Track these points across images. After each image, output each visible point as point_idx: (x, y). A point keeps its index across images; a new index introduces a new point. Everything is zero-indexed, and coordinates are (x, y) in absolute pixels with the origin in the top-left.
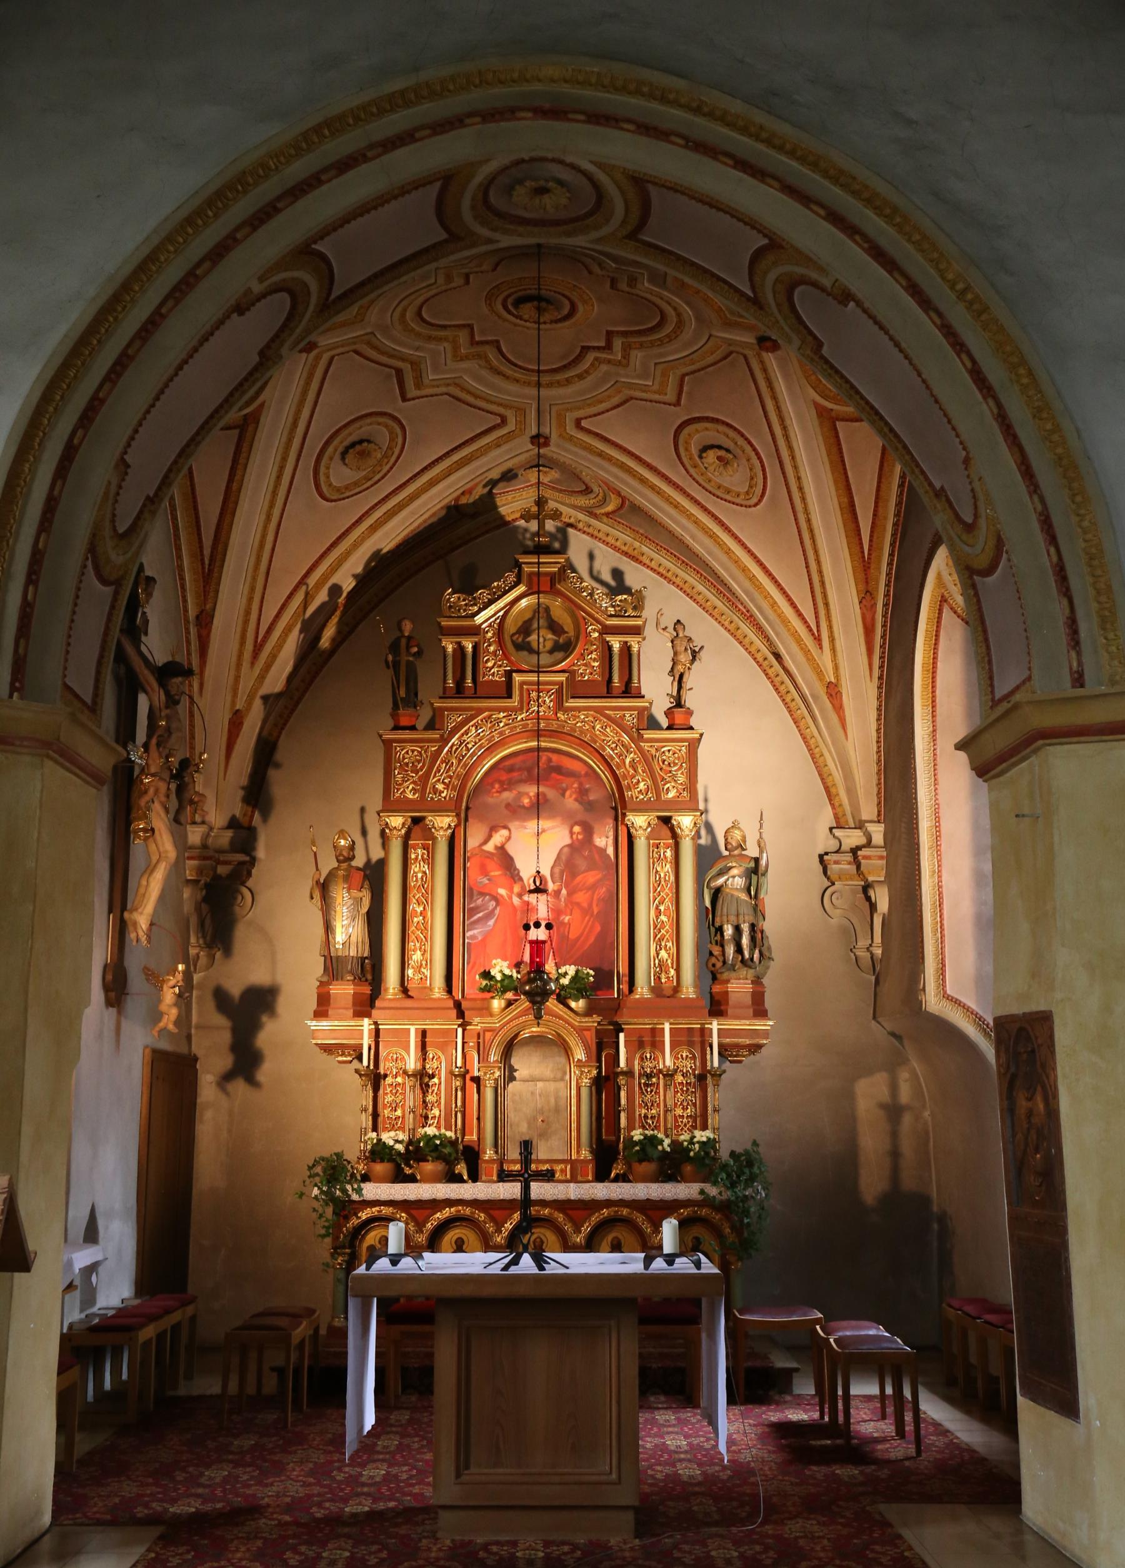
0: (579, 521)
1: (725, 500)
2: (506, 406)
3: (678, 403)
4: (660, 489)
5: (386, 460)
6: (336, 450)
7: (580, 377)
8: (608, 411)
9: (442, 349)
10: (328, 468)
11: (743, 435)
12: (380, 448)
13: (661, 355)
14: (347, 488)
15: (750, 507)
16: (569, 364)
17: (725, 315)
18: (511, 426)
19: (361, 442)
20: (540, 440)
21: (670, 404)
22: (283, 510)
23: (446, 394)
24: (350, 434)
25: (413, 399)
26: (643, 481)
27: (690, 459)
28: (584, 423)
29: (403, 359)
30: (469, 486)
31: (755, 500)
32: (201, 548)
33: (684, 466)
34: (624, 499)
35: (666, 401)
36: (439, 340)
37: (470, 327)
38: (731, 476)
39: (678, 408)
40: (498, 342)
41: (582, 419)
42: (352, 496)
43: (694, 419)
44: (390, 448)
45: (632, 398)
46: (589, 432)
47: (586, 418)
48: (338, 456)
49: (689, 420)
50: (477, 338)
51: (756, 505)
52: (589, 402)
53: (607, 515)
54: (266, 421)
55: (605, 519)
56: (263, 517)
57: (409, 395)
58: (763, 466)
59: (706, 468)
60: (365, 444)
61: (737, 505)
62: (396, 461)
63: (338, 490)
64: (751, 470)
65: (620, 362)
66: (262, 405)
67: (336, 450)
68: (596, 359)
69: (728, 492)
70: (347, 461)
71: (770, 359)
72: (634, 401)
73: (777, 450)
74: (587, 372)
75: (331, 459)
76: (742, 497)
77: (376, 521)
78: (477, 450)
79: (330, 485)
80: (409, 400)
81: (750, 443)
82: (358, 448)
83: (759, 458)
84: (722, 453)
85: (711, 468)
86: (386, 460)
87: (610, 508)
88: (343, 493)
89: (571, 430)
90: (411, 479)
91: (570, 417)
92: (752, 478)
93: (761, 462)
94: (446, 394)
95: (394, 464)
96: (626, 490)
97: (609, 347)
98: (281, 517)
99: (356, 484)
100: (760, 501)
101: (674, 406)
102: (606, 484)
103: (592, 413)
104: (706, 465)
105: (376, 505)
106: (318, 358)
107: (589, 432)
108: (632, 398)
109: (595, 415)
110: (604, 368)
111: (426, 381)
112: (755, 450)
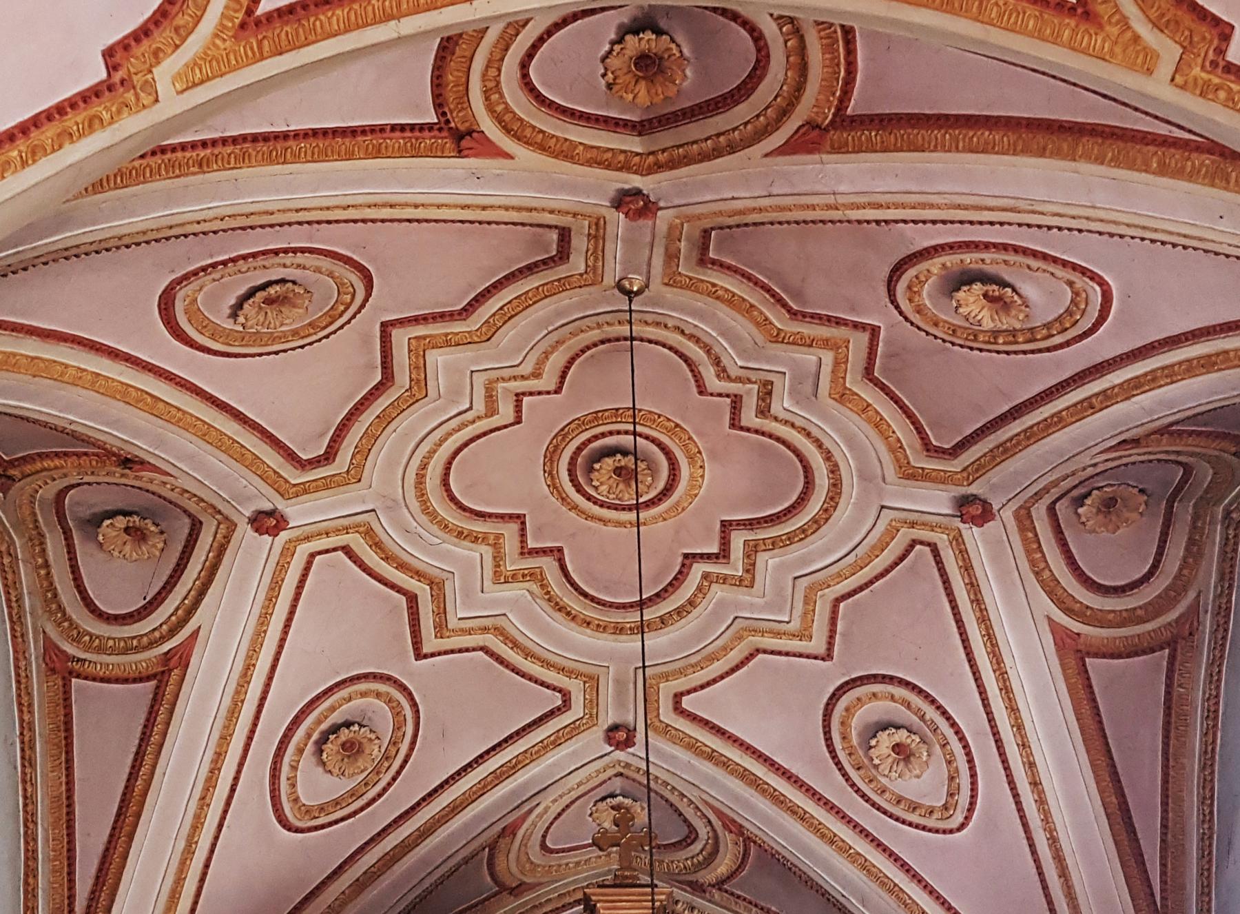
0: (677, 902)
1: (910, 824)
2: (569, 673)
3: (828, 656)
4: (805, 812)
5: (386, 764)
6: (309, 736)
7: (680, 612)
8: (722, 677)
9: (478, 555)
10: (294, 768)
11: (933, 701)
12: (378, 738)
13: (805, 561)
14: (322, 808)
15: (951, 831)
16: (665, 590)
17: (906, 457)
18: (577, 711)
19: (348, 724)
20: (619, 736)
21: (816, 658)
22: (216, 838)
23: (482, 649)
24: (332, 709)
25: (433, 655)
26: (778, 799)
27: (850, 754)
28: (686, 703)
29: (418, 574)
30: (510, 819)
31: (959, 818)
32: (71, 898)
33: (841, 769)
34: (748, 840)
35: (809, 651)
36: (475, 538)
37: (520, 519)
38: (918, 777)
39: (828, 663)
40: (560, 550)
41: (682, 694)
42: (330, 824)
43: (854, 680)
44: (394, 743)
45: (758, 651)
46: (693, 718)
47: (689, 692)
48: (310, 747)
49: (847, 683)
50: (531, 544)
51: (962, 826)
52: (693, 660)
53: (720, 884)
54: (200, 663)
55: (717, 895)
56: (182, 844)
57: (426, 649)
58: (968, 754)
59: (876, 767)
60: (356, 727)
61: (930, 830)
62: (402, 767)
63: (308, 811)
64: (949, 762)
65: (741, 579)
66: (195, 633)
67: (309, 736)
68: (706, 576)
69: (914, 807)
70: (324, 756)
71: (973, 536)
72: (760, 656)
73: (991, 720)
74: (691, 603)
75: (300, 751)
76: (937, 815)
77: (365, 873)
78: (525, 752)
79: (296, 800)
80: (426, 656)
81: (944, 713)
82: (345, 734)
83: (962, 739)
84: (901, 736)
85: (884, 768)
86: (386, 764)
87: (723, 866)
88: (315, 818)
89: (667, 715)
90: (424, 799)
91: (666, 690)
92: (951, 779)
93: (966, 747)
94: (482, 649)
95: (398, 773)
96: (752, 823)
97: (724, 554)
98: (212, 851)
99: (337, 803)
100: (967, 819)
101: (823, 659)
102: (720, 814)
103: (699, 683)
104: (876, 761)
105: (367, 843)
106: (288, 551)
107: (693, 718)
108: (758, 651)
109: (702, 687)
110: (718, 592)
111: (453, 623)
112: (953, 724)
